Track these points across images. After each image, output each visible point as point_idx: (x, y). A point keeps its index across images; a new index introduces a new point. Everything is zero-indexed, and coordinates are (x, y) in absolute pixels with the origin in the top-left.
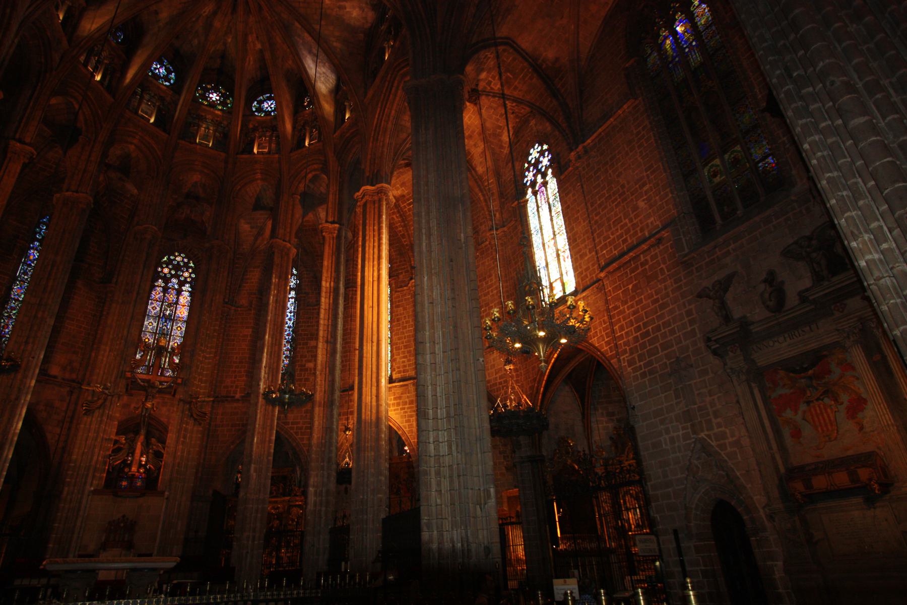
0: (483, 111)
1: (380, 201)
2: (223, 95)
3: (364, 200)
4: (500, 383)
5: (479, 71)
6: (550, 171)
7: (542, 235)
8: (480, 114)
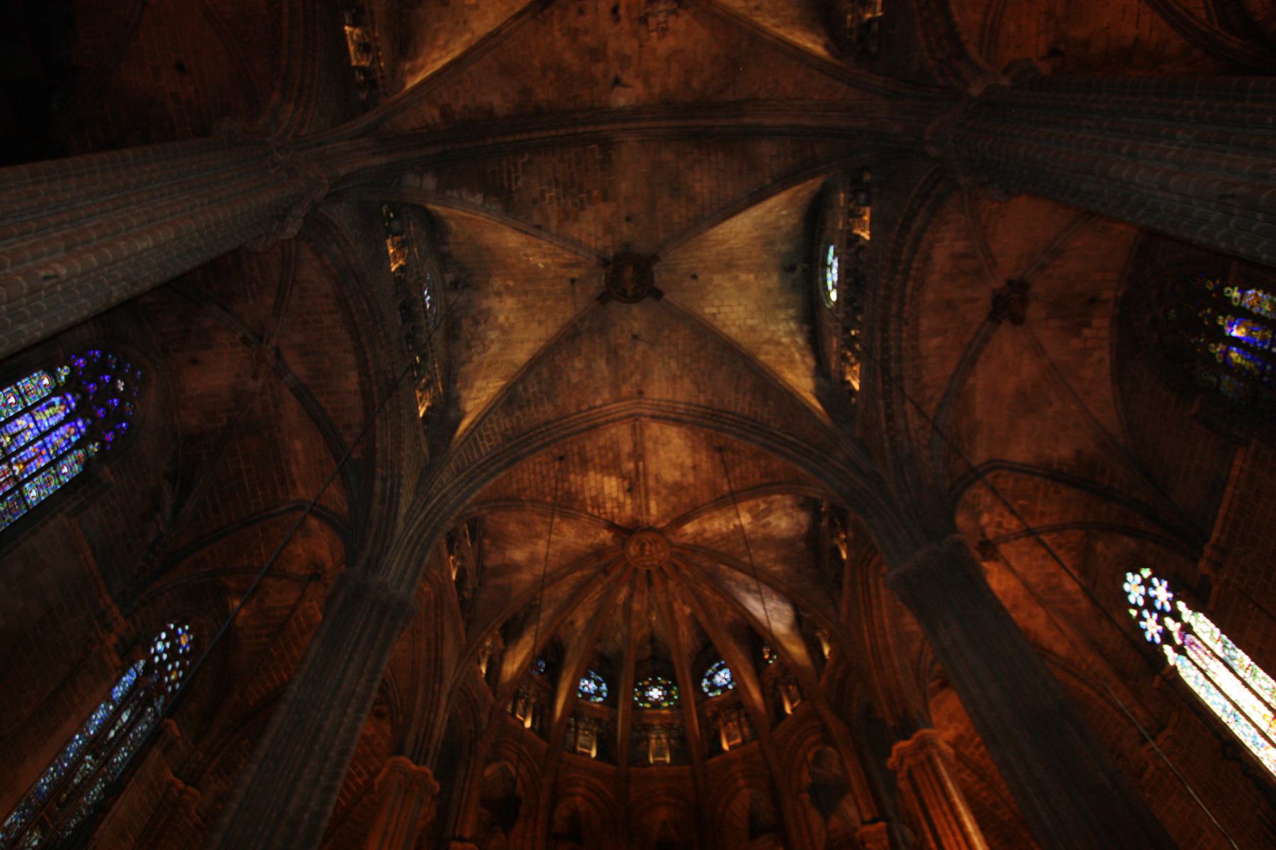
0: (1013, 563)
1: (930, 759)
2: (667, 688)
3: (905, 767)
5: (976, 516)
6: (1181, 606)
7: (1248, 718)
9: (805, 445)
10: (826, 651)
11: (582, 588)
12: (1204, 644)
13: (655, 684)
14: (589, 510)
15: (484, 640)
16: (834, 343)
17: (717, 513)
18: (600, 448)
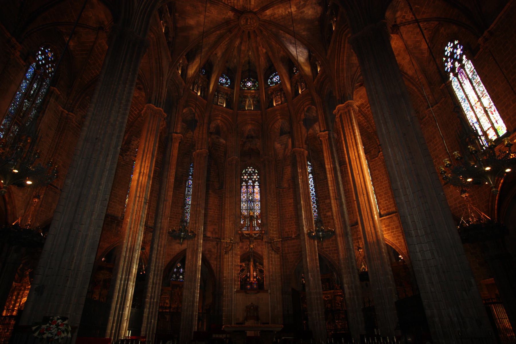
0: (404, 36)
1: (349, 111)
2: (254, 82)
3: (339, 113)
4: (460, 207)
6: (464, 57)
7: (469, 101)
8: (402, 38)
12: (466, 73)
13: (249, 81)
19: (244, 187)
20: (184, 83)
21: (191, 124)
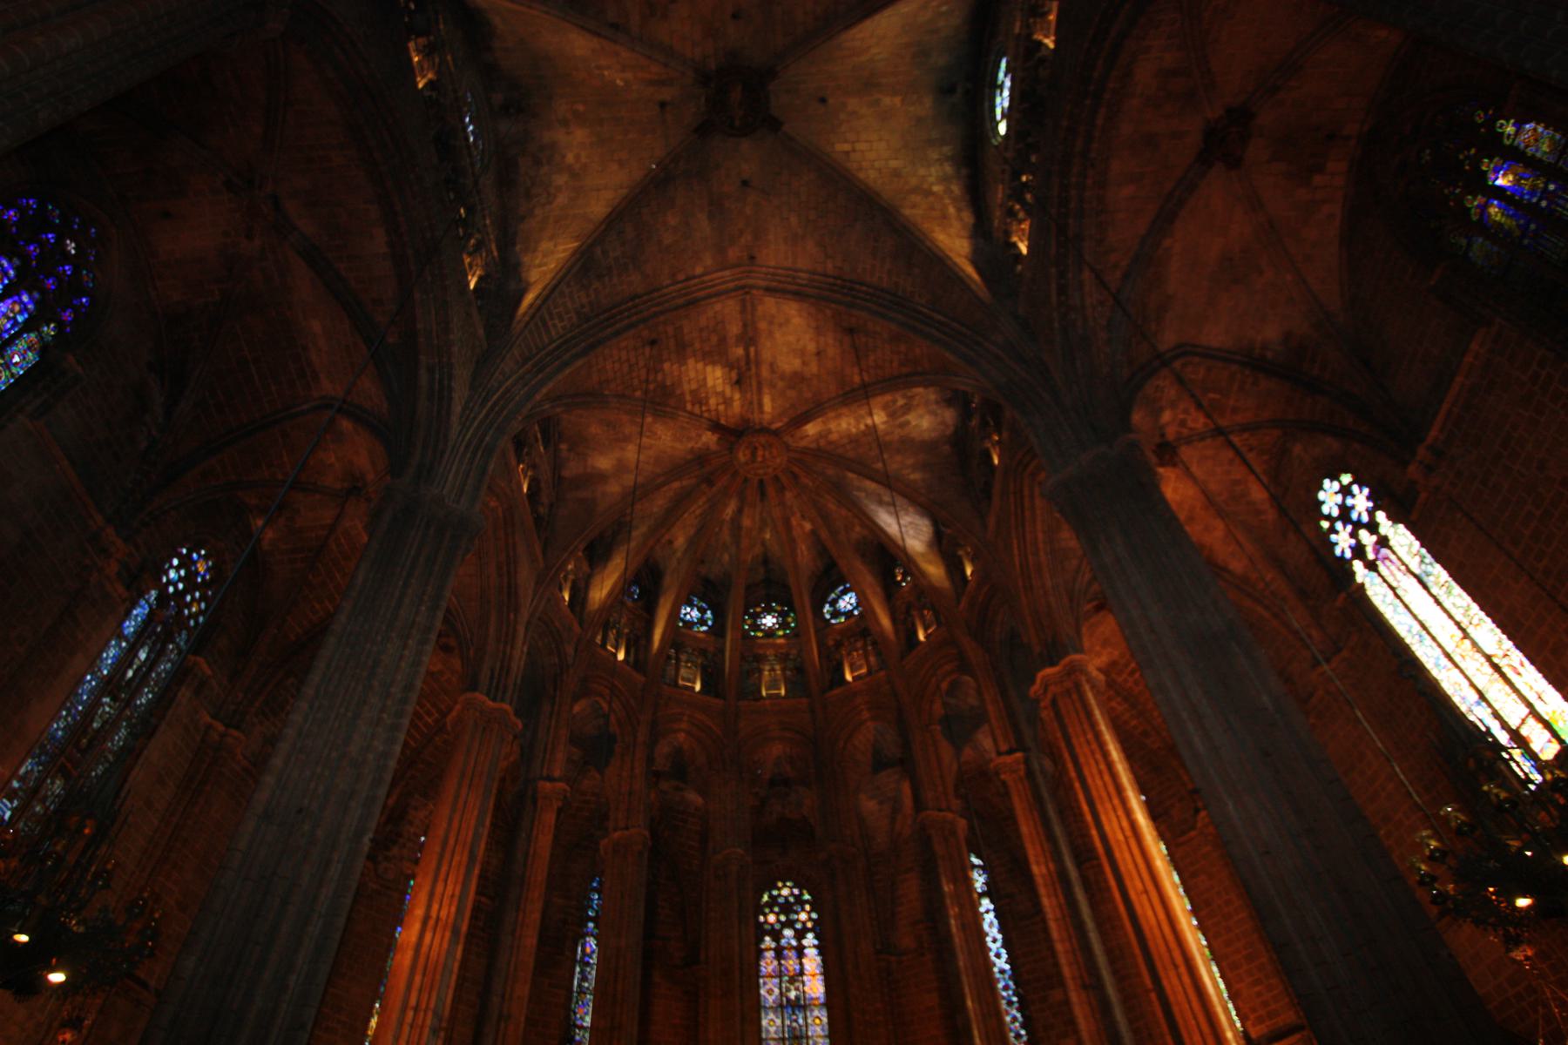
0: (1194, 469)
1: (1078, 686)
2: (783, 614)
3: (1049, 696)
6: (1381, 516)
7: (1434, 639)
9: (955, 325)
10: (969, 571)
11: (680, 503)
13: (769, 610)
14: (689, 407)
15: (566, 562)
16: (999, 193)
17: (845, 410)
18: (701, 330)
19: (770, 954)
20: (577, 629)
21: (595, 750)
